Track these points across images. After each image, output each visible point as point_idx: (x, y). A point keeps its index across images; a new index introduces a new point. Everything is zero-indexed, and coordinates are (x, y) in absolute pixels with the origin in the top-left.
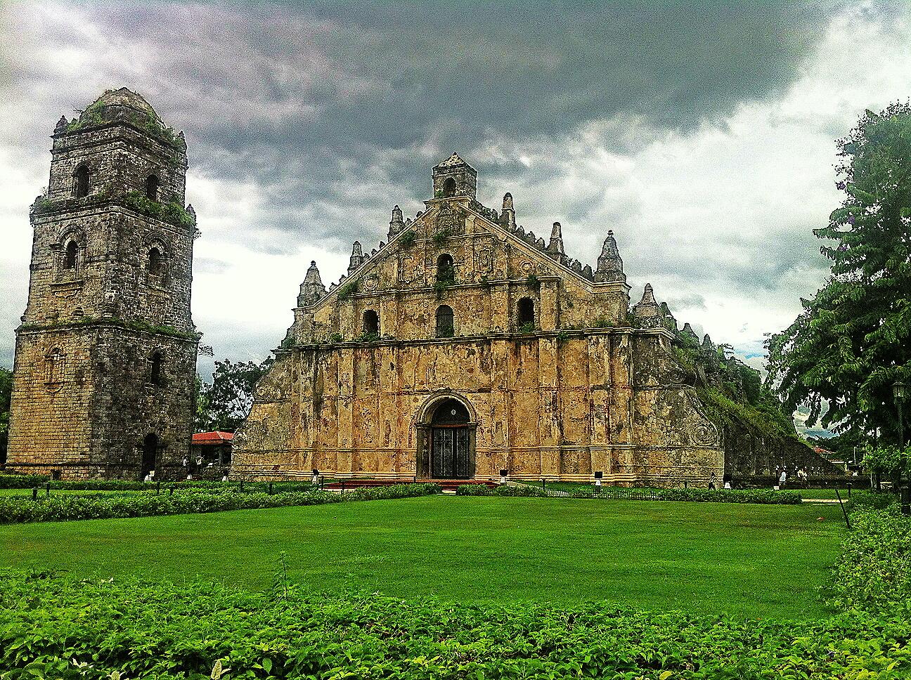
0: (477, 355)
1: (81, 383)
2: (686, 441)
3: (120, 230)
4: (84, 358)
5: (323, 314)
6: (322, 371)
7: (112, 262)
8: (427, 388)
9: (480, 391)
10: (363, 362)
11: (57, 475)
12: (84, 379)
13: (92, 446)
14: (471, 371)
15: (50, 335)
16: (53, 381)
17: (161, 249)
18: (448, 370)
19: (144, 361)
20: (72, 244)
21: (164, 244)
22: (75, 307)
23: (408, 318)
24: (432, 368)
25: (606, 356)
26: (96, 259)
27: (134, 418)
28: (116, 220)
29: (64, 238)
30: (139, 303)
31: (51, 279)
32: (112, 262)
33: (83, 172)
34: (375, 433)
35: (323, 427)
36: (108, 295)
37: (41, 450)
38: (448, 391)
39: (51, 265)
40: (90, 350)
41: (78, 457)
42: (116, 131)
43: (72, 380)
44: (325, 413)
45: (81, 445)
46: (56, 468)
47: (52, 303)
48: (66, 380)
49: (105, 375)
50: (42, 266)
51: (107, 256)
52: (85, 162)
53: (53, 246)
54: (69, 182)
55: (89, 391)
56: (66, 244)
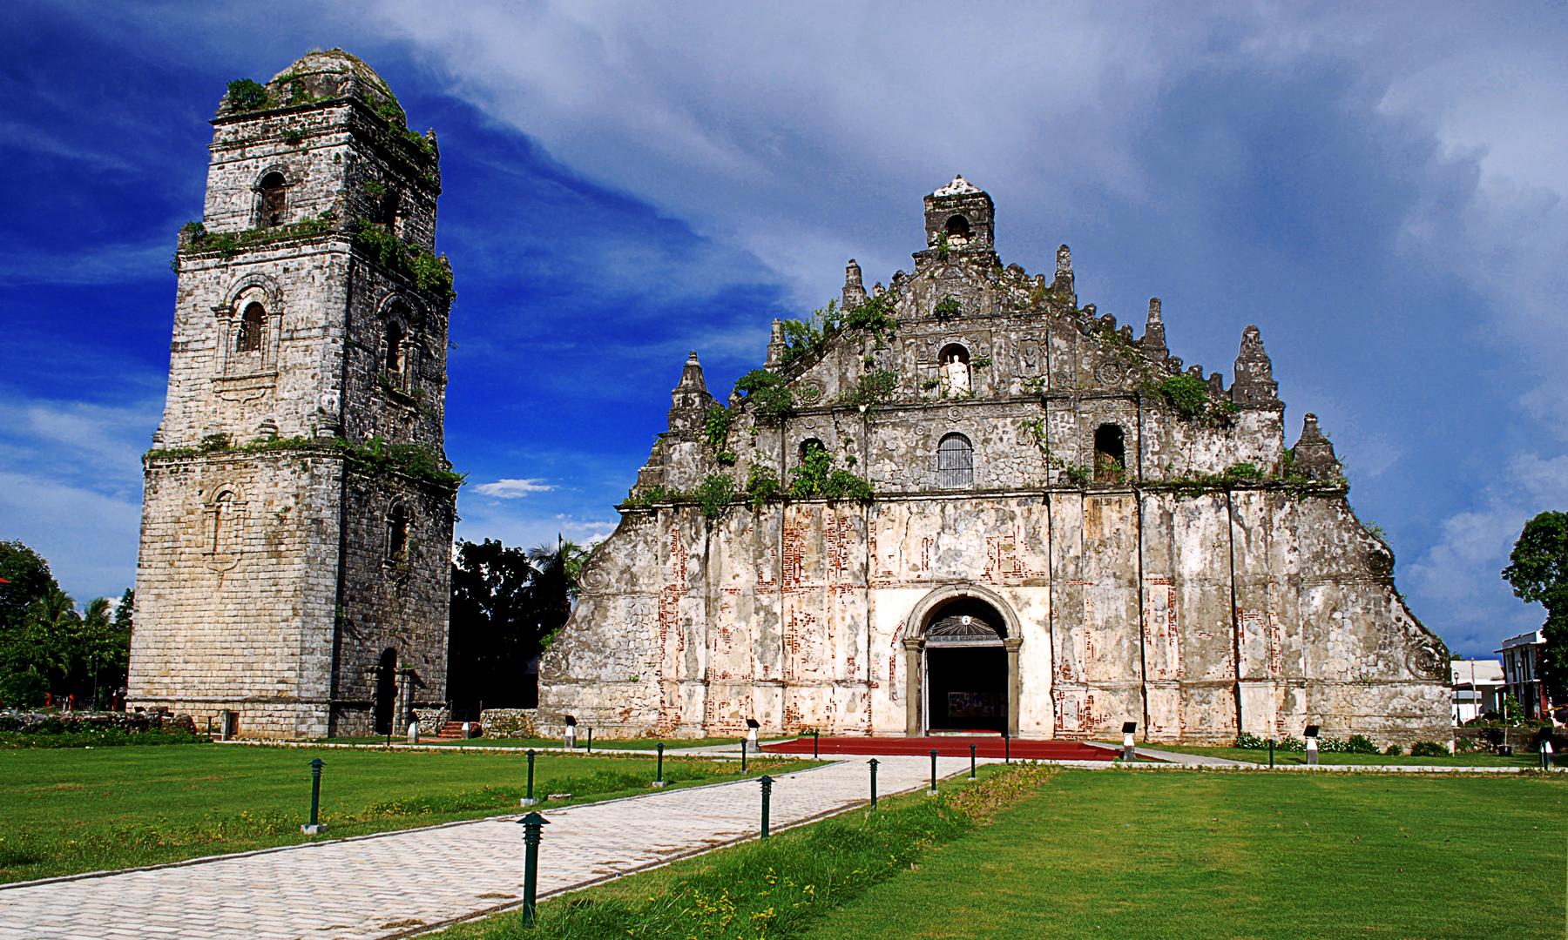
0: (1019, 521)
1: (279, 555)
2: (1396, 671)
3: (349, 285)
6: (717, 543)
7: (334, 341)
8: (925, 575)
9: (1027, 584)
11: (232, 718)
12: (283, 548)
14: (1011, 547)
15: (213, 468)
16: (220, 549)
18: (970, 550)
20: (255, 311)
22: (261, 420)
26: (303, 334)
28: (341, 267)
29: (238, 297)
32: (334, 341)
33: (272, 185)
34: (829, 653)
35: (721, 643)
36: (326, 398)
37: (197, 673)
38: (963, 581)
39: (212, 343)
40: (296, 496)
41: (272, 688)
42: (340, 114)
43: (260, 548)
44: (727, 619)
45: (279, 666)
46: (228, 706)
48: (246, 549)
49: (324, 542)
50: (199, 346)
51: (325, 328)
52: (277, 165)
54: (247, 200)
55: (293, 569)
56: (242, 306)
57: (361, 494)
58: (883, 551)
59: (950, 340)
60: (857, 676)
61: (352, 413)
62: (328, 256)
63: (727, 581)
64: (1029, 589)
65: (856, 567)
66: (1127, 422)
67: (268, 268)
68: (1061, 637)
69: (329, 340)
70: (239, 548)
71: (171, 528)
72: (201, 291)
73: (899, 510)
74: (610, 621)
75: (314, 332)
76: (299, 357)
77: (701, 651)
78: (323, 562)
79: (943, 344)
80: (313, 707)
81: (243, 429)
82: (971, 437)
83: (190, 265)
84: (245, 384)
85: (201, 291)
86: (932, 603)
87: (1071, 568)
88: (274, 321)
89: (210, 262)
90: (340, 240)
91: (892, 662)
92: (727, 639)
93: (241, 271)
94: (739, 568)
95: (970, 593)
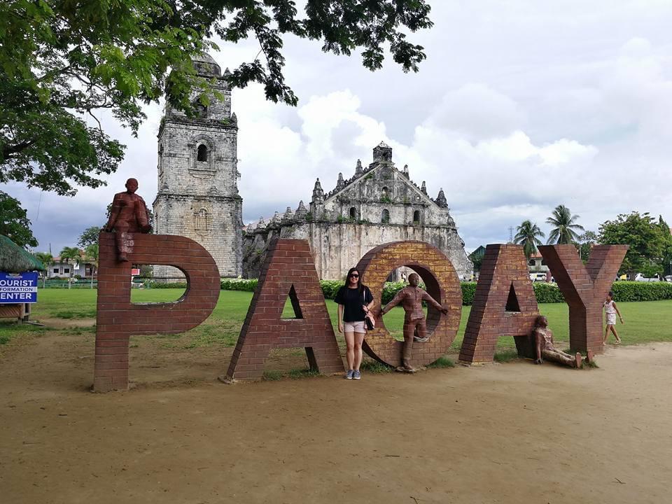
4: (226, 217)
5: (330, 205)
10: (350, 231)
13: (237, 267)
22: (210, 186)
23: (371, 213)
24: (382, 236)
25: (446, 236)
31: (185, 165)
44: (332, 253)
45: (228, 266)
47: (190, 181)
50: (180, 156)
53: (189, 145)
55: (231, 236)
56: (198, 145)
59: (385, 186)
62: (232, 135)
63: (332, 244)
66: (421, 210)
67: (207, 133)
70: (210, 229)
71: (180, 220)
72: (179, 136)
73: (374, 227)
75: (229, 160)
76: (224, 167)
77: (328, 261)
81: (201, 188)
83: (174, 125)
84: (202, 173)
85: (179, 136)
88: (213, 153)
89: (182, 126)
92: (332, 258)
93: (197, 133)
94: (336, 240)
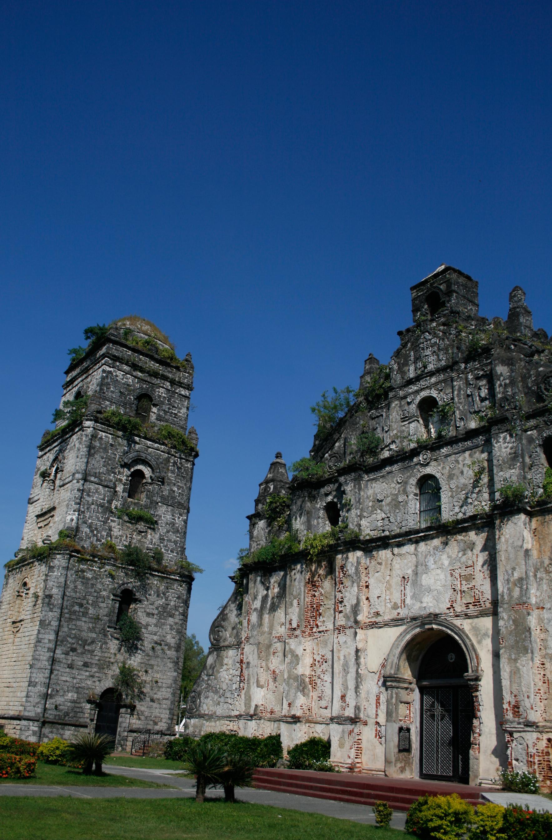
7: (78, 482)
8: (403, 613)
17: (147, 472)
19: (108, 597)
21: (150, 466)
27: (86, 665)
28: (87, 436)
30: (110, 530)
32: (78, 482)
36: (69, 518)
57: (88, 579)
58: (374, 592)
60: (346, 714)
61: (90, 527)
64: (482, 619)
65: (348, 609)
68: (508, 670)
69: (75, 481)
74: (225, 667)
78: (49, 624)
79: (418, 398)
80: (31, 723)
82: (438, 475)
86: (408, 637)
87: (516, 592)
90: (87, 420)
91: (378, 699)
95: (434, 626)
